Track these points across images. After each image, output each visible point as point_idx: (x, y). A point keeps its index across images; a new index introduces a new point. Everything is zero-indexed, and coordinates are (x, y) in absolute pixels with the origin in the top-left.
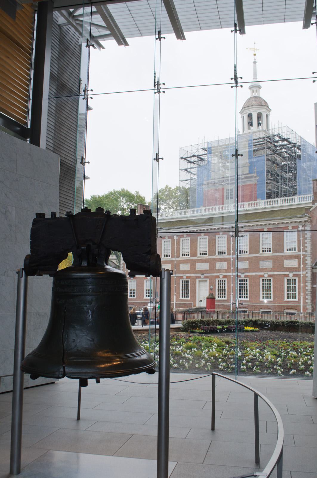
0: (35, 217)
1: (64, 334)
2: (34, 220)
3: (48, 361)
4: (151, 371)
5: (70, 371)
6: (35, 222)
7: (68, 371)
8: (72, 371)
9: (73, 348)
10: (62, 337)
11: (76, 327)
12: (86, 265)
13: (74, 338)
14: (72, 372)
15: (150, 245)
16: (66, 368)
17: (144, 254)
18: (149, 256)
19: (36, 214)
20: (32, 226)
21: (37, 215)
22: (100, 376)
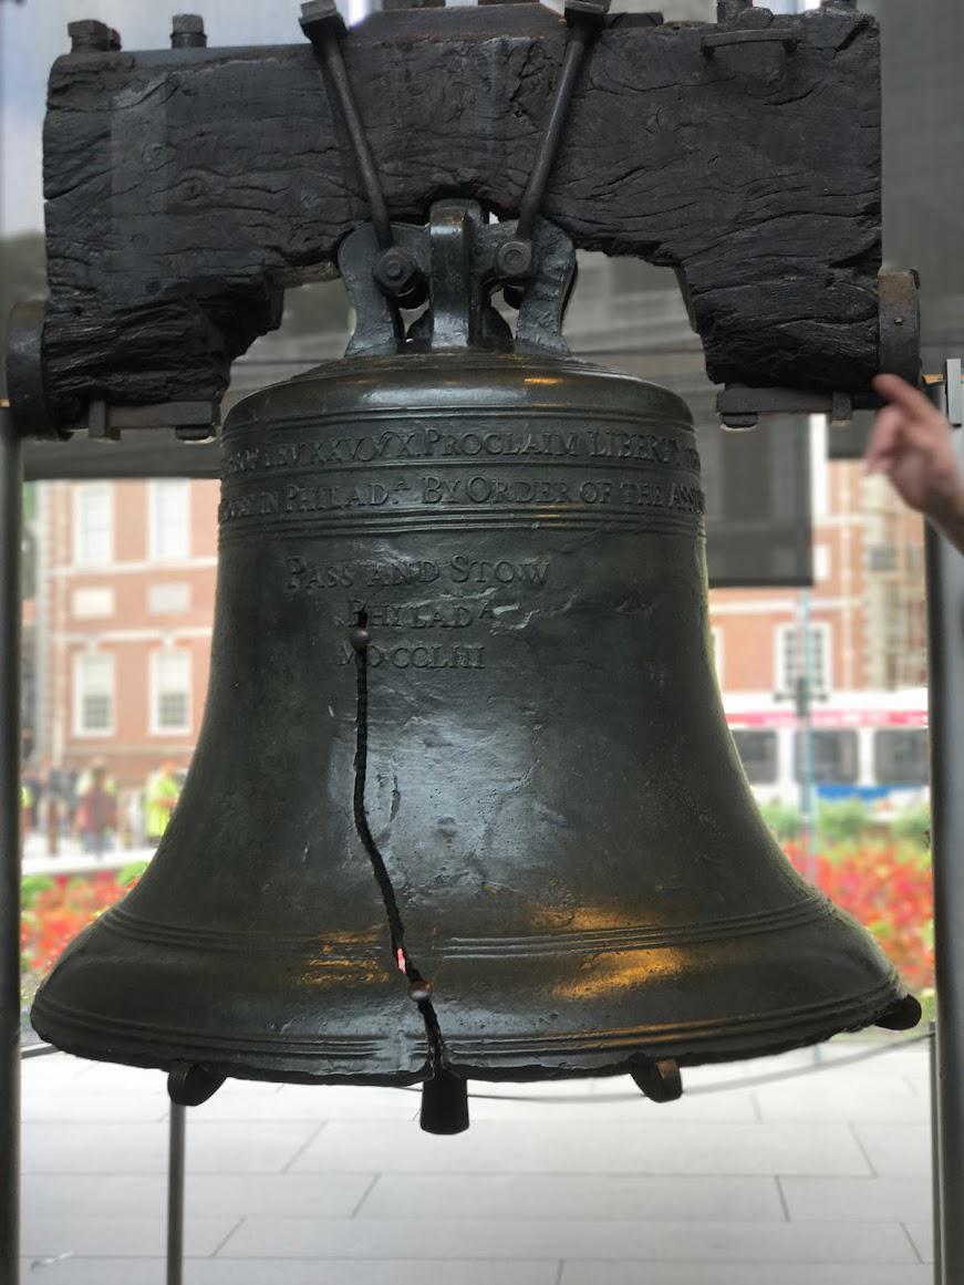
0: (64, 46)
1: (371, 784)
2: (59, 69)
3: (200, 983)
4: (901, 1014)
5: (473, 1032)
6: (65, 85)
7: (463, 1031)
8: (488, 1030)
9: (456, 878)
10: (361, 812)
11: (448, 736)
12: (461, 341)
13: (447, 815)
14: (489, 1037)
15: (874, 211)
16: (437, 1008)
17: (837, 272)
18: (864, 280)
19: (76, 30)
20: (48, 104)
21: (76, 30)
22: (681, 1051)
